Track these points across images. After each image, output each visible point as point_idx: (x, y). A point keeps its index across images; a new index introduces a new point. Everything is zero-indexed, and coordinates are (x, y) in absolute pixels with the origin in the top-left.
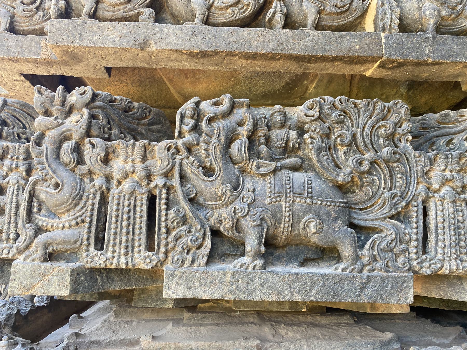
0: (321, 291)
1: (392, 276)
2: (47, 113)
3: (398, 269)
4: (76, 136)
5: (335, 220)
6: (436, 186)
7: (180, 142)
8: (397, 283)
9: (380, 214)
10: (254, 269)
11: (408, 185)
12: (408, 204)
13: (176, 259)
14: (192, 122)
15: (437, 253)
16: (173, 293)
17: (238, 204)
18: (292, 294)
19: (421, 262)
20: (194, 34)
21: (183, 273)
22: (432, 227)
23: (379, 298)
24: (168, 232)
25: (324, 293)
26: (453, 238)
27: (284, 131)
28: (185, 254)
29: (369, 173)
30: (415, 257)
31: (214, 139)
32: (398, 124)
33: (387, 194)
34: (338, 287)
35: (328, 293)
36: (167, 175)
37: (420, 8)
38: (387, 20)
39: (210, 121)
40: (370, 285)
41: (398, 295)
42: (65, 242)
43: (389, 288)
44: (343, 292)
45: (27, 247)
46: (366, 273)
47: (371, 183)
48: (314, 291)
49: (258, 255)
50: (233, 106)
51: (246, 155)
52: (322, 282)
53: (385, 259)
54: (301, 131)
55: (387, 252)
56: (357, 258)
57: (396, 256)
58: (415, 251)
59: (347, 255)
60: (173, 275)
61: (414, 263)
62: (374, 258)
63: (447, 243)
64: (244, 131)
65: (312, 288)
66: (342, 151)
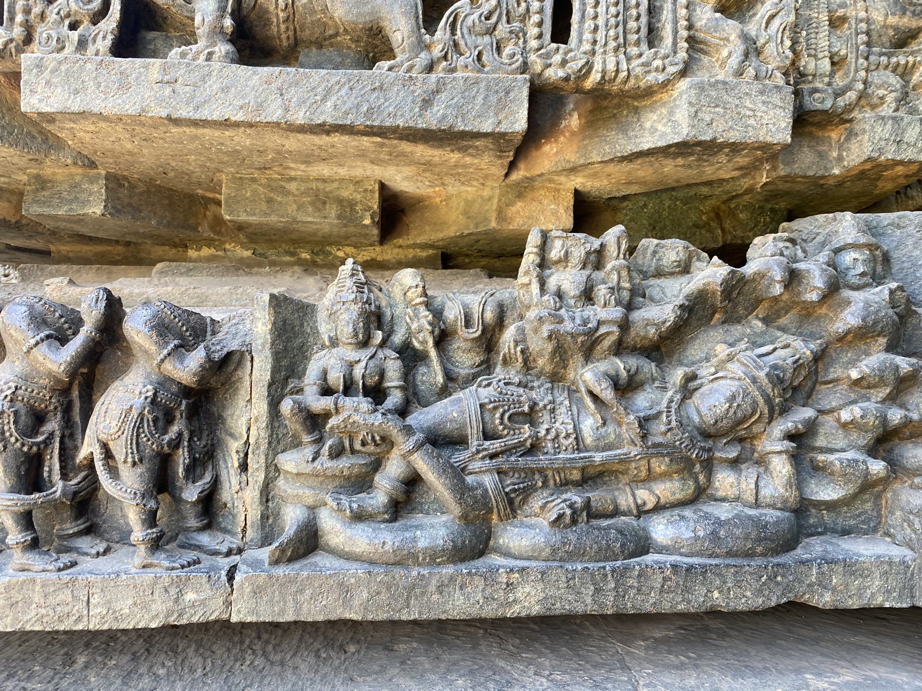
0: (345, 103)
1: (487, 78)
8: (497, 92)
10: (208, 59)
13: (45, 35)
15: (580, 41)
16: (40, 101)
18: (287, 110)
19: (548, 56)
21: (60, 63)
23: (459, 119)
25: (350, 109)
26: (613, 10)
28: (66, 28)
30: (534, 44)
34: (378, 98)
35: (358, 106)
40: (443, 96)
41: (496, 114)
43: (480, 100)
44: (389, 106)
48: (329, 104)
49: (217, 31)
52: (347, 87)
53: (476, 47)
55: (482, 35)
58: (535, 31)
59: (400, 38)
60: (40, 66)
61: (533, 57)
63: (601, 21)
65: (325, 99)
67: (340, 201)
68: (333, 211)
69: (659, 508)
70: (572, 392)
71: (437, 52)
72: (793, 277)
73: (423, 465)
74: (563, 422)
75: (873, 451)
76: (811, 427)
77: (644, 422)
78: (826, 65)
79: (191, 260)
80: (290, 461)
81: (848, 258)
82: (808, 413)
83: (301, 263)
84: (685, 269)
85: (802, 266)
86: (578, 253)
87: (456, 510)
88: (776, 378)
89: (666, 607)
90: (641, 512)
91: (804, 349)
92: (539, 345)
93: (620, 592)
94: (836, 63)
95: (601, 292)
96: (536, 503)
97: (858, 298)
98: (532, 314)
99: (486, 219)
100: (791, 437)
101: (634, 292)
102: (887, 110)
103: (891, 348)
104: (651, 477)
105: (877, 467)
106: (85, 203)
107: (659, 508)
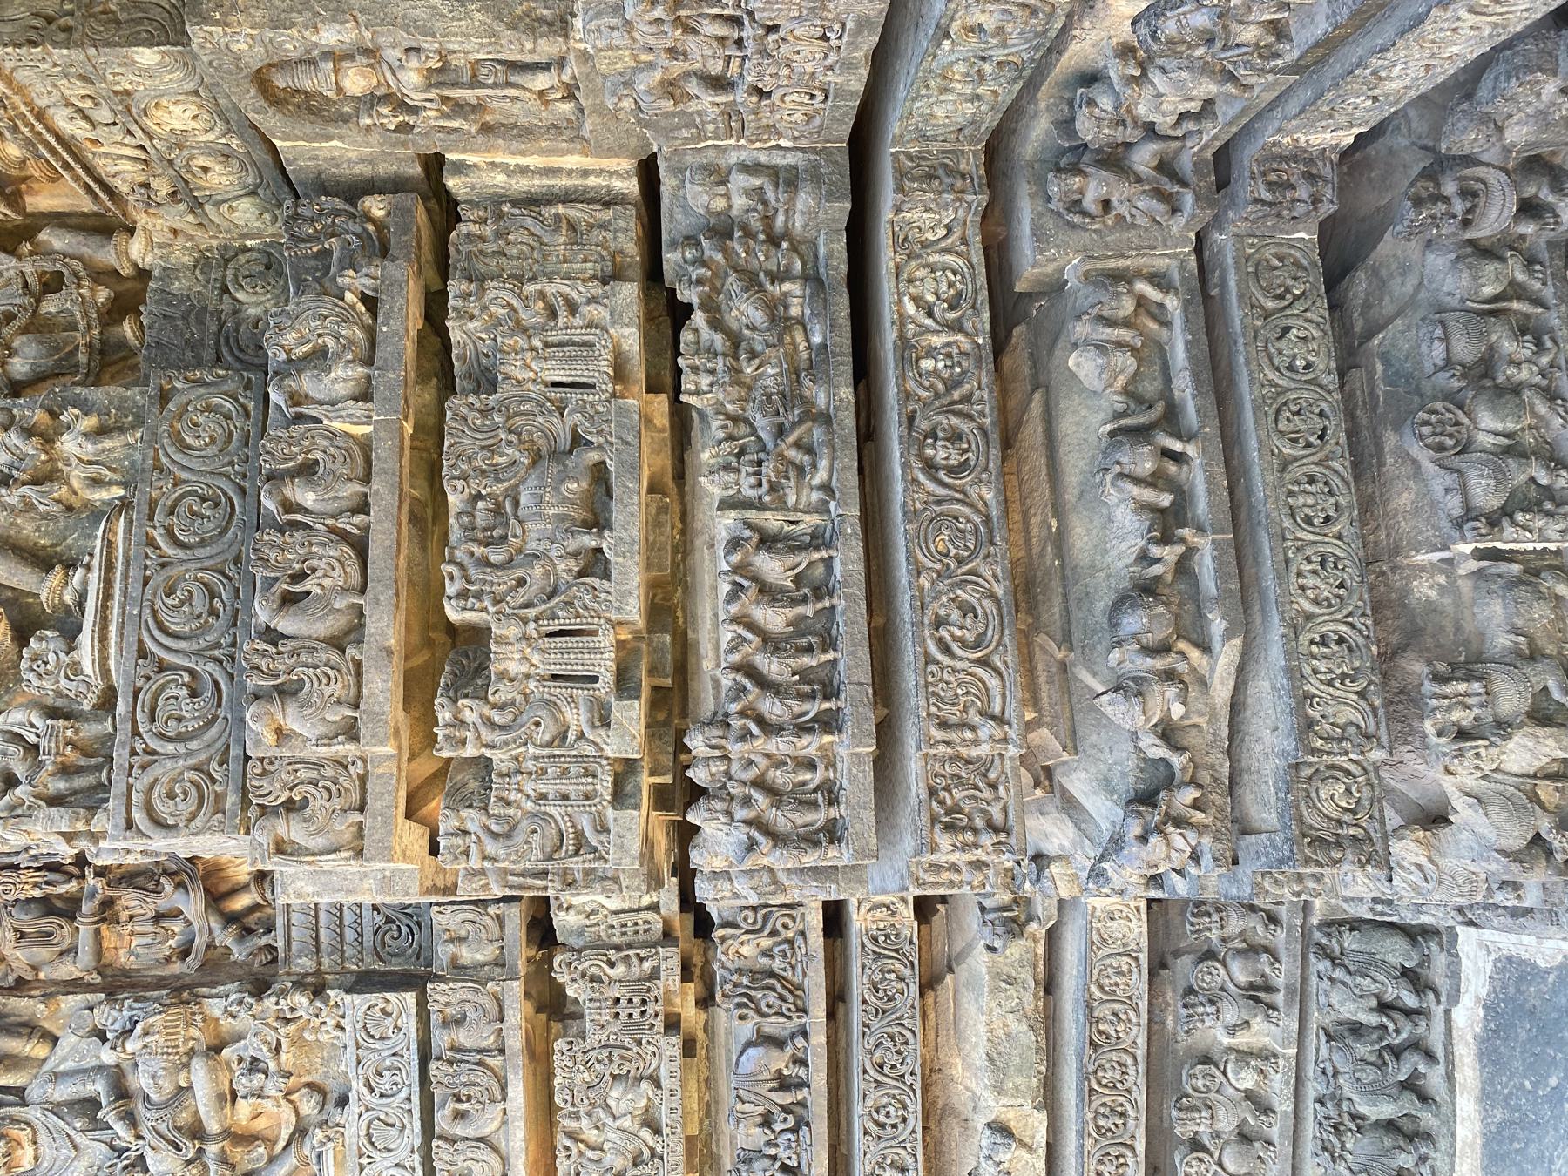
2: (463, 742)
3: (609, 412)
4: (486, 710)
5: (565, 466)
6: (531, 374)
7: (492, 609)
9: (560, 426)
11: (531, 400)
12: (549, 400)
14: (471, 599)
17: (553, 554)
20: (377, 602)
22: (570, 379)
24: (578, 616)
27: (477, 513)
29: (519, 434)
31: (489, 578)
32: (471, 406)
33: (540, 419)
36: (525, 621)
37: (345, 380)
38: (358, 413)
39: (469, 582)
42: (591, 710)
45: (596, 744)
46: (614, 440)
47: (530, 433)
49: (600, 535)
50: (452, 561)
51: (505, 547)
54: (479, 496)
56: (600, 447)
57: (597, 412)
60: (619, 609)
62: (600, 433)
64: (478, 550)
66: (497, 459)
67: (658, 514)
68: (663, 517)
69: (808, 340)
70: (757, 378)
71: (602, 440)
72: (699, 282)
73: (791, 439)
74: (770, 382)
75: (778, 246)
76: (768, 273)
77: (768, 346)
78: (589, 265)
79: (685, 622)
80: (792, 499)
81: (688, 255)
82: (762, 275)
83: (684, 559)
84: (696, 331)
85: (694, 278)
86: (693, 377)
87: (809, 424)
88: (747, 289)
89: (849, 335)
90: (809, 348)
91: (732, 277)
92: (735, 392)
93: (842, 354)
94: (585, 261)
95: (709, 365)
96: (807, 393)
97: (707, 253)
98: (721, 396)
99: (664, 439)
100: (773, 283)
101: (708, 351)
102: (610, 235)
103: (731, 239)
104: (793, 343)
105: (785, 245)
106: (664, 644)
107: (808, 340)
